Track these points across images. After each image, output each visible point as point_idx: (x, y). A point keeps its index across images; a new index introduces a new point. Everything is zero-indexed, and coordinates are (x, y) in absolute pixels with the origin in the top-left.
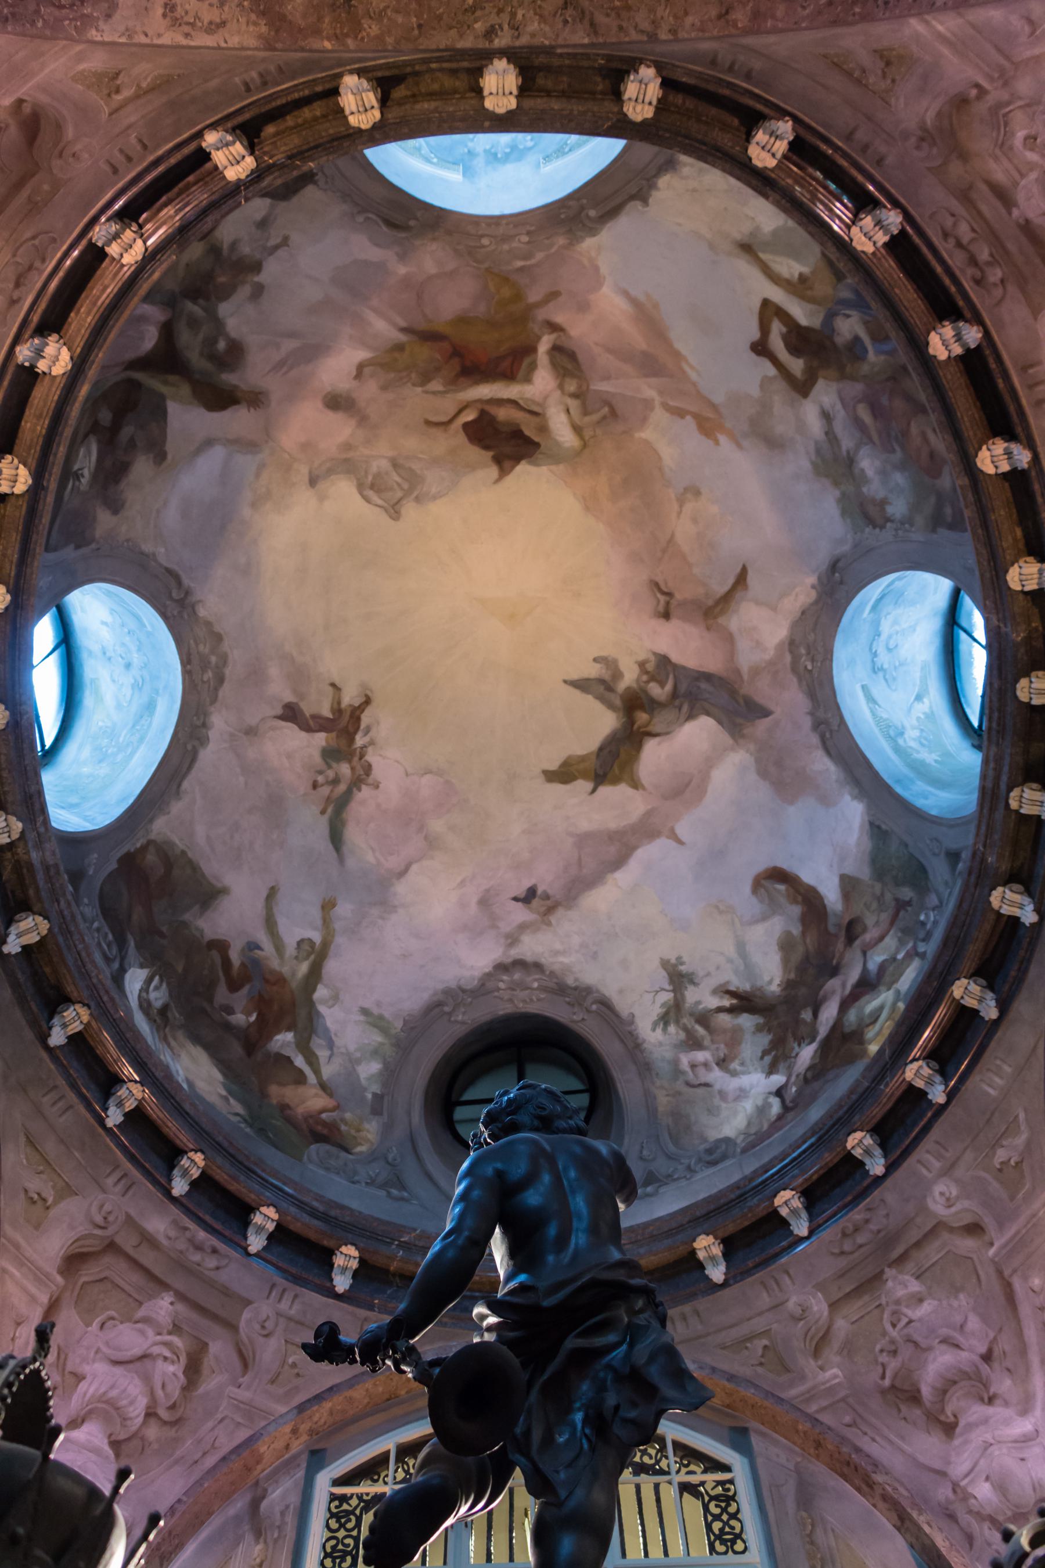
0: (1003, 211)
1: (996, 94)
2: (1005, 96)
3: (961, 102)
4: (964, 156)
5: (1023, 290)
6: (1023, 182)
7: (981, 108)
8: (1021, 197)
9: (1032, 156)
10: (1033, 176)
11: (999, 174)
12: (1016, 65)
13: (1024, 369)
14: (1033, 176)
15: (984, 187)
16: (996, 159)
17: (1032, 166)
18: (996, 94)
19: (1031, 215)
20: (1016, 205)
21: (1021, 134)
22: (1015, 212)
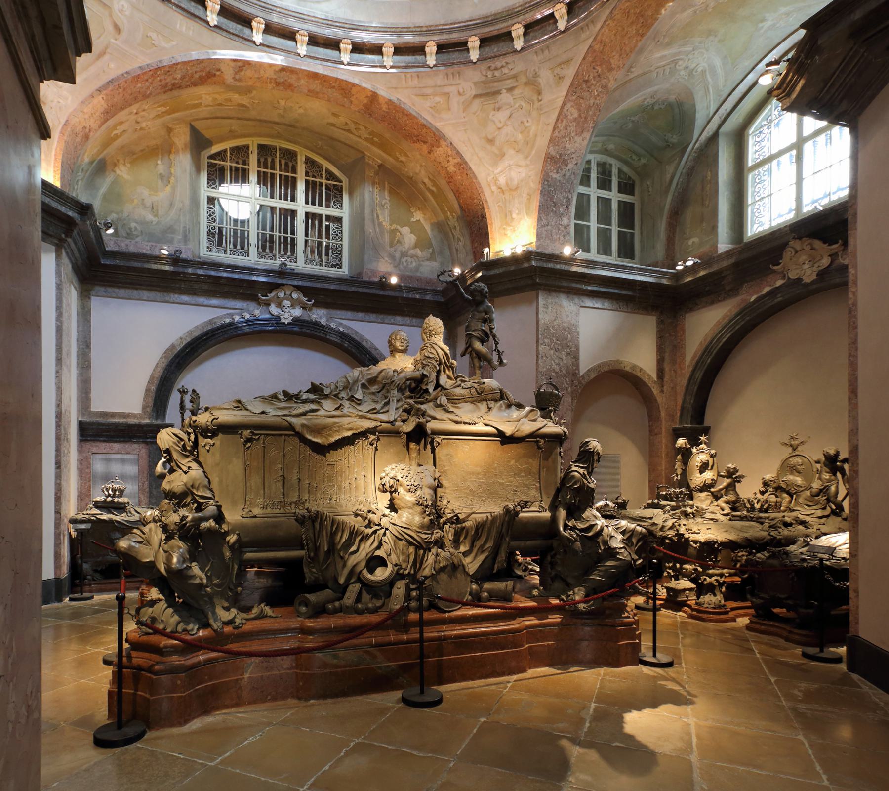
0: (507, 87)
1: (537, 104)
2: (535, 107)
3: (539, 93)
5: (482, 82)
6: (512, 98)
7: (535, 98)
8: (508, 95)
9: (517, 105)
10: (512, 102)
11: (516, 92)
12: (540, 114)
13: (459, 73)
14: (512, 102)
16: (521, 94)
18: (537, 104)
19: (502, 95)
20: (507, 92)
21: (524, 105)
22: (504, 91)
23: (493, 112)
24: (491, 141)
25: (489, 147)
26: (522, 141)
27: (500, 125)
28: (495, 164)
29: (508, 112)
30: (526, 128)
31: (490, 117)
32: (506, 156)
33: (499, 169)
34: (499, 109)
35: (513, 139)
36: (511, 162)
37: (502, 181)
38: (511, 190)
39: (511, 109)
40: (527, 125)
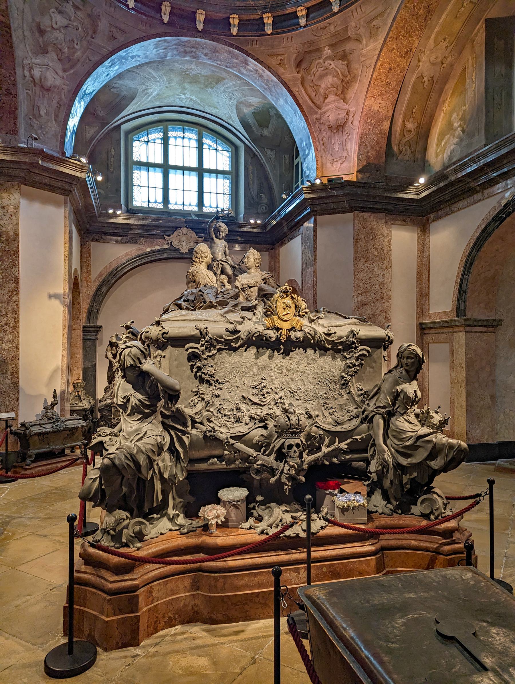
4: (89, 16)
15: (81, 7)
17: (74, 21)
23: (53, 10)
24: (42, 32)
25: (37, 34)
26: (66, 55)
27: (55, 26)
28: (36, 53)
29: (65, 22)
30: (74, 48)
31: (51, 11)
32: (48, 55)
33: (38, 61)
34: (60, 12)
35: (59, 46)
36: (51, 64)
37: (37, 73)
38: (42, 87)
39: (69, 22)
40: (76, 46)
